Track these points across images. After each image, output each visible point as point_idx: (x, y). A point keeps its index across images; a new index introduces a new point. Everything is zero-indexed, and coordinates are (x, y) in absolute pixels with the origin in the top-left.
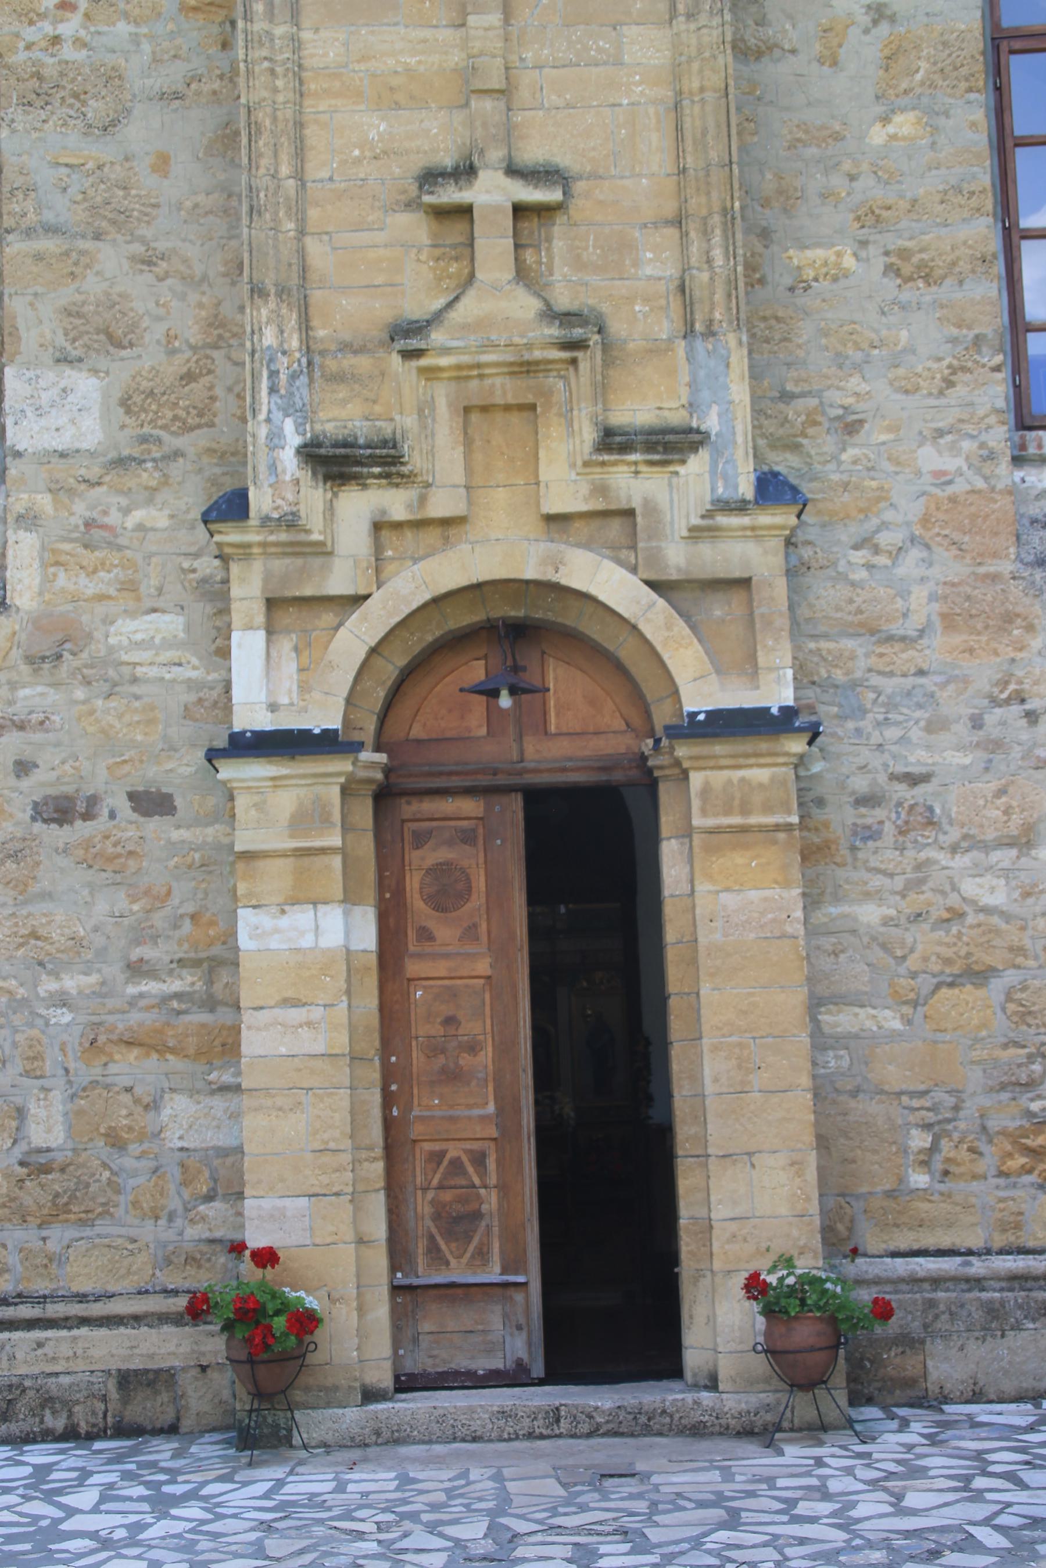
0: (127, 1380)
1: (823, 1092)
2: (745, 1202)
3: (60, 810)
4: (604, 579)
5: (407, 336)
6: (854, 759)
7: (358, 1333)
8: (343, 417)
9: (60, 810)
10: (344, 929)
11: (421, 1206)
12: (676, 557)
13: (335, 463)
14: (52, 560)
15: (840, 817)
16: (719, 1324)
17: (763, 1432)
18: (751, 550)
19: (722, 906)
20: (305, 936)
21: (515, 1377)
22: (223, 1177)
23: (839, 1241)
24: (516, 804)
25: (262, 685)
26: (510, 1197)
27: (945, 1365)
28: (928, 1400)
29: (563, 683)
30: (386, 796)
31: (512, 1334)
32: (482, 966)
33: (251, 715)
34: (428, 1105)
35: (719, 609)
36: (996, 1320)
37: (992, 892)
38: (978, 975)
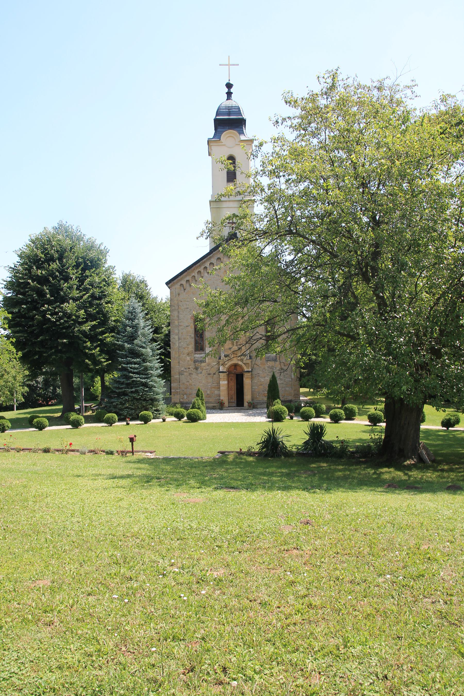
0: (213, 406)
1: (252, 391)
2: (247, 397)
3: (209, 374)
4: (240, 363)
5: (230, 349)
6: (254, 372)
7: (226, 404)
8: (226, 353)
9: (209, 374)
10: (226, 382)
11: (230, 398)
12: (245, 362)
13: (226, 356)
14: (208, 359)
15: (254, 376)
16: (246, 404)
17: (248, 410)
18: (249, 361)
19: (247, 381)
20: (224, 383)
21: (235, 407)
22: (219, 396)
23: (252, 400)
24: (235, 375)
25: (221, 369)
26: (235, 397)
27: (258, 406)
28: (257, 408)
29: (238, 367)
30: (228, 375)
31: (235, 404)
32: (233, 384)
33: (221, 370)
34: (230, 392)
35: (247, 365)
36: (261, 404)
37: (263, 380)
38: (262, 385)
